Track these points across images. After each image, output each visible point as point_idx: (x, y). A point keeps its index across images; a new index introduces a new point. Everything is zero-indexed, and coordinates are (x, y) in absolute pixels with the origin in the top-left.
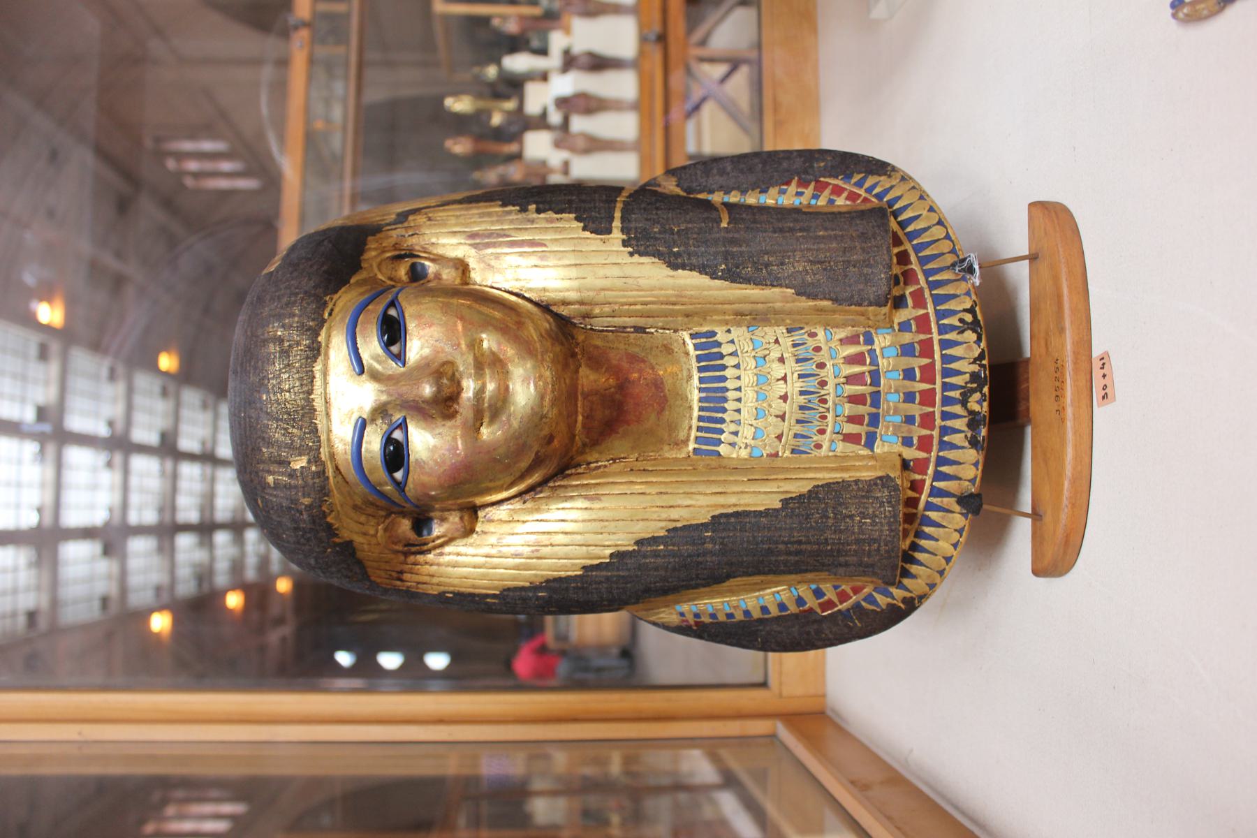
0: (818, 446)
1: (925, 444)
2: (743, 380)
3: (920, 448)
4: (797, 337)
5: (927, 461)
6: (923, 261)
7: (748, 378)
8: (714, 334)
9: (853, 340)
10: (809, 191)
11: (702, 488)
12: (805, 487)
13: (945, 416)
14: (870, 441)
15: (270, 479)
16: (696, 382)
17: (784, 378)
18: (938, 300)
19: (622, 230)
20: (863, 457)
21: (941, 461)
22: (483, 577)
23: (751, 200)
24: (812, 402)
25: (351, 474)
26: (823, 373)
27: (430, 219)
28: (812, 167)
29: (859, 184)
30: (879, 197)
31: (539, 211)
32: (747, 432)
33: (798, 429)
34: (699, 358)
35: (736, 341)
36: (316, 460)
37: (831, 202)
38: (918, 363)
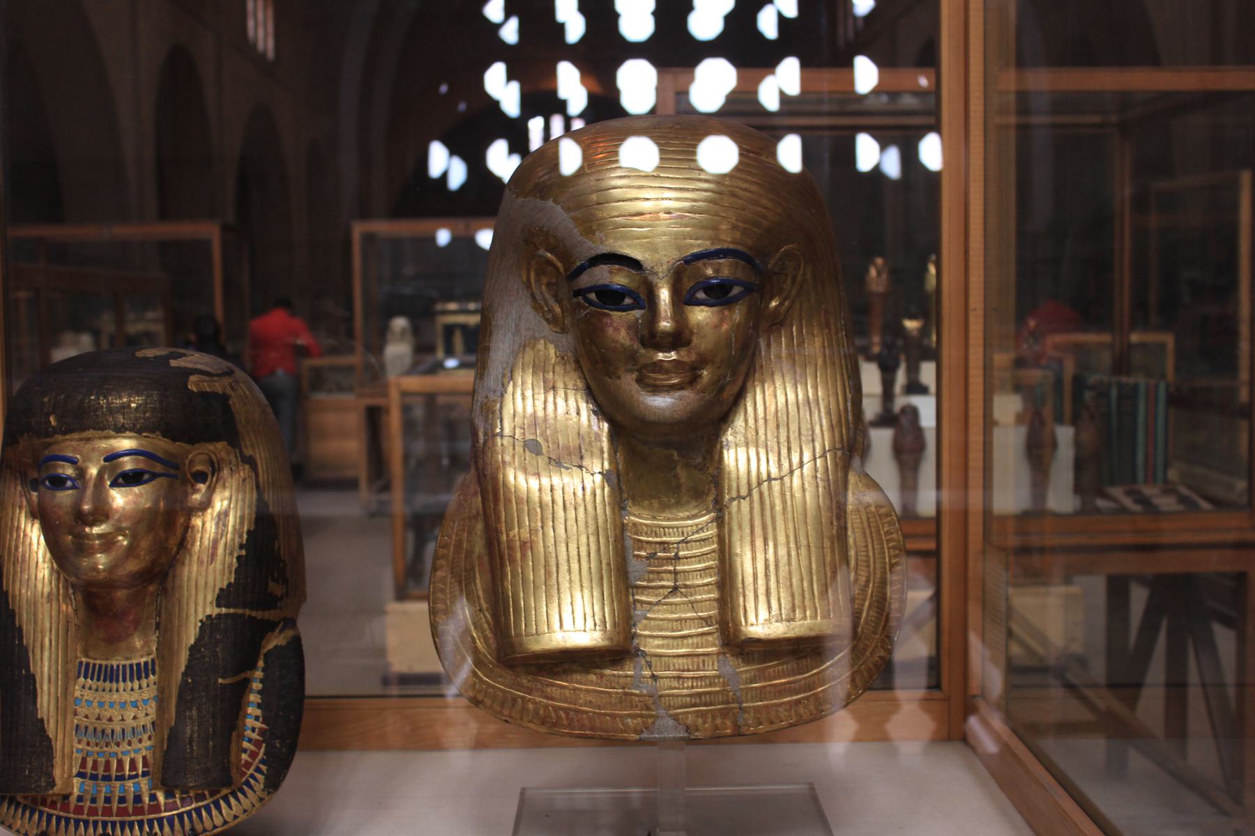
0: (79, 742)
1: (79, 810)
2: (126, 692)
3: (76, 807)
4: (149, 727)
5: (69, 812)
6: (198, 810)
7: (126, 697)
8: (154, 674)
9: (145, 764)
10: (255, 736)
11: (53, 667)
12: (51, 734)
13: (95, 824)
14: (80, 775)
15: (46, 400)
16: (123, 663)
17: (123, 720)
18: (170, 820)
19: (219, 616)
20: (71, 770)
21: (68, 820)
22: (6, 524)
23: (254, 698)
24: (103, 736)
25: (55, 450)
26: (125, 744)
27: (244, 480)
28: (277, 738)
29: (258, 770)
30: (247, 783)
31: (239, 558)
32: (88, 695)
33: (91, 729)
34: (138, 665)
35: (147, 690)
36: (56, 431)
37: (245, 751)
38: (130, 805)
